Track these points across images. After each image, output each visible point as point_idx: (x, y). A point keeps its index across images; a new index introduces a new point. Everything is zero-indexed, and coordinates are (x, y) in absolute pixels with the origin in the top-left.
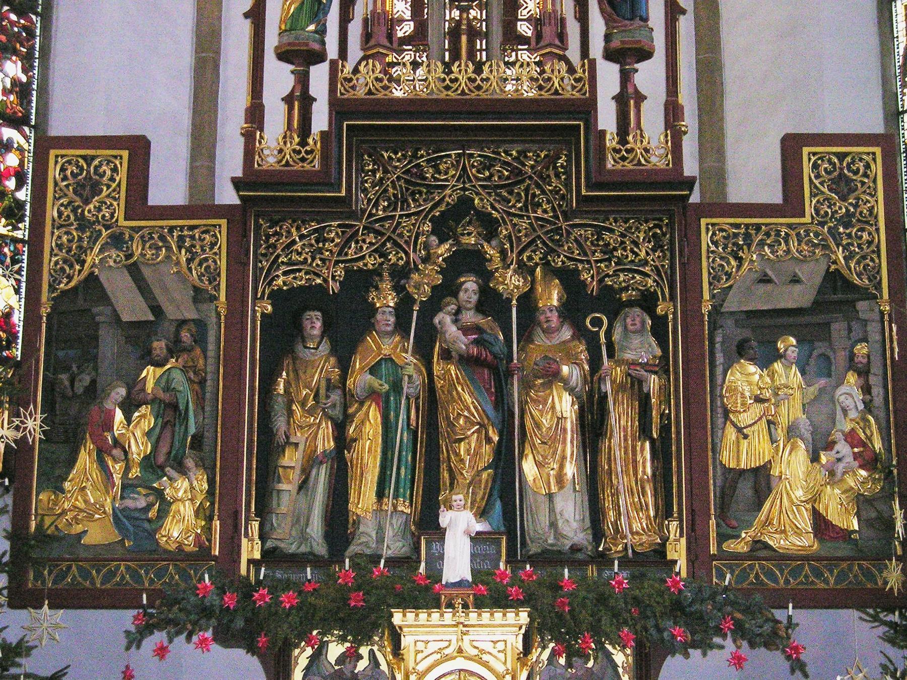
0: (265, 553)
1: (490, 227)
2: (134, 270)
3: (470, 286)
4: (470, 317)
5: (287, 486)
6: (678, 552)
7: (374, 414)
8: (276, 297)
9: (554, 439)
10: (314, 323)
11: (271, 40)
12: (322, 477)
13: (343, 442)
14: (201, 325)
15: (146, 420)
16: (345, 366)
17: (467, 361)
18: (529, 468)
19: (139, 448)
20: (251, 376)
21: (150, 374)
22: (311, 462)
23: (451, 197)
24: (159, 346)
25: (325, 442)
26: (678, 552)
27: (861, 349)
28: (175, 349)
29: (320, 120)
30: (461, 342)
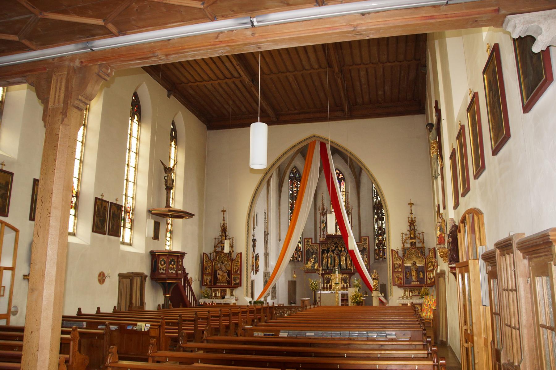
0: (323, 269)
1: (338, 244)
2: (312, 248)
3: (337, 249)
4: (337, 251)
5: (324, 264)
6: (352, 269)
7: (330, 259)
8: (322, 250)
9: (343, 260)
10: (325, 252)
11: (321, 230)
12: (326, 263)
13: (328, 261)
14: (317, 252)
15: (313, 259)
16: (328, 255)
17: (337, 255)
18: (341, 263)
19: (313, 262)
20: (321, 256)
21: (313, 256)
22: (325, 263)
23: (335, 242)
24: (314, 254)
25: (326, 261)
26: (352, 269)
27: (366, 253)
28: (315, 254)
29: (325, 237)
30: (336, 253)
